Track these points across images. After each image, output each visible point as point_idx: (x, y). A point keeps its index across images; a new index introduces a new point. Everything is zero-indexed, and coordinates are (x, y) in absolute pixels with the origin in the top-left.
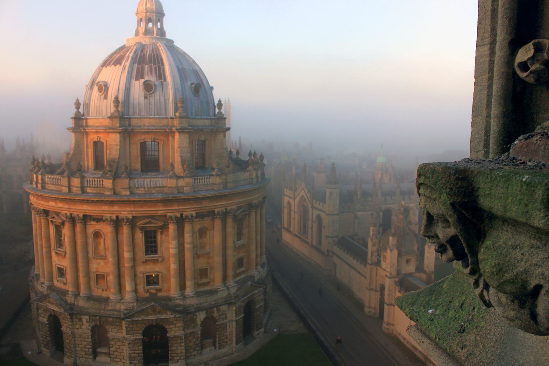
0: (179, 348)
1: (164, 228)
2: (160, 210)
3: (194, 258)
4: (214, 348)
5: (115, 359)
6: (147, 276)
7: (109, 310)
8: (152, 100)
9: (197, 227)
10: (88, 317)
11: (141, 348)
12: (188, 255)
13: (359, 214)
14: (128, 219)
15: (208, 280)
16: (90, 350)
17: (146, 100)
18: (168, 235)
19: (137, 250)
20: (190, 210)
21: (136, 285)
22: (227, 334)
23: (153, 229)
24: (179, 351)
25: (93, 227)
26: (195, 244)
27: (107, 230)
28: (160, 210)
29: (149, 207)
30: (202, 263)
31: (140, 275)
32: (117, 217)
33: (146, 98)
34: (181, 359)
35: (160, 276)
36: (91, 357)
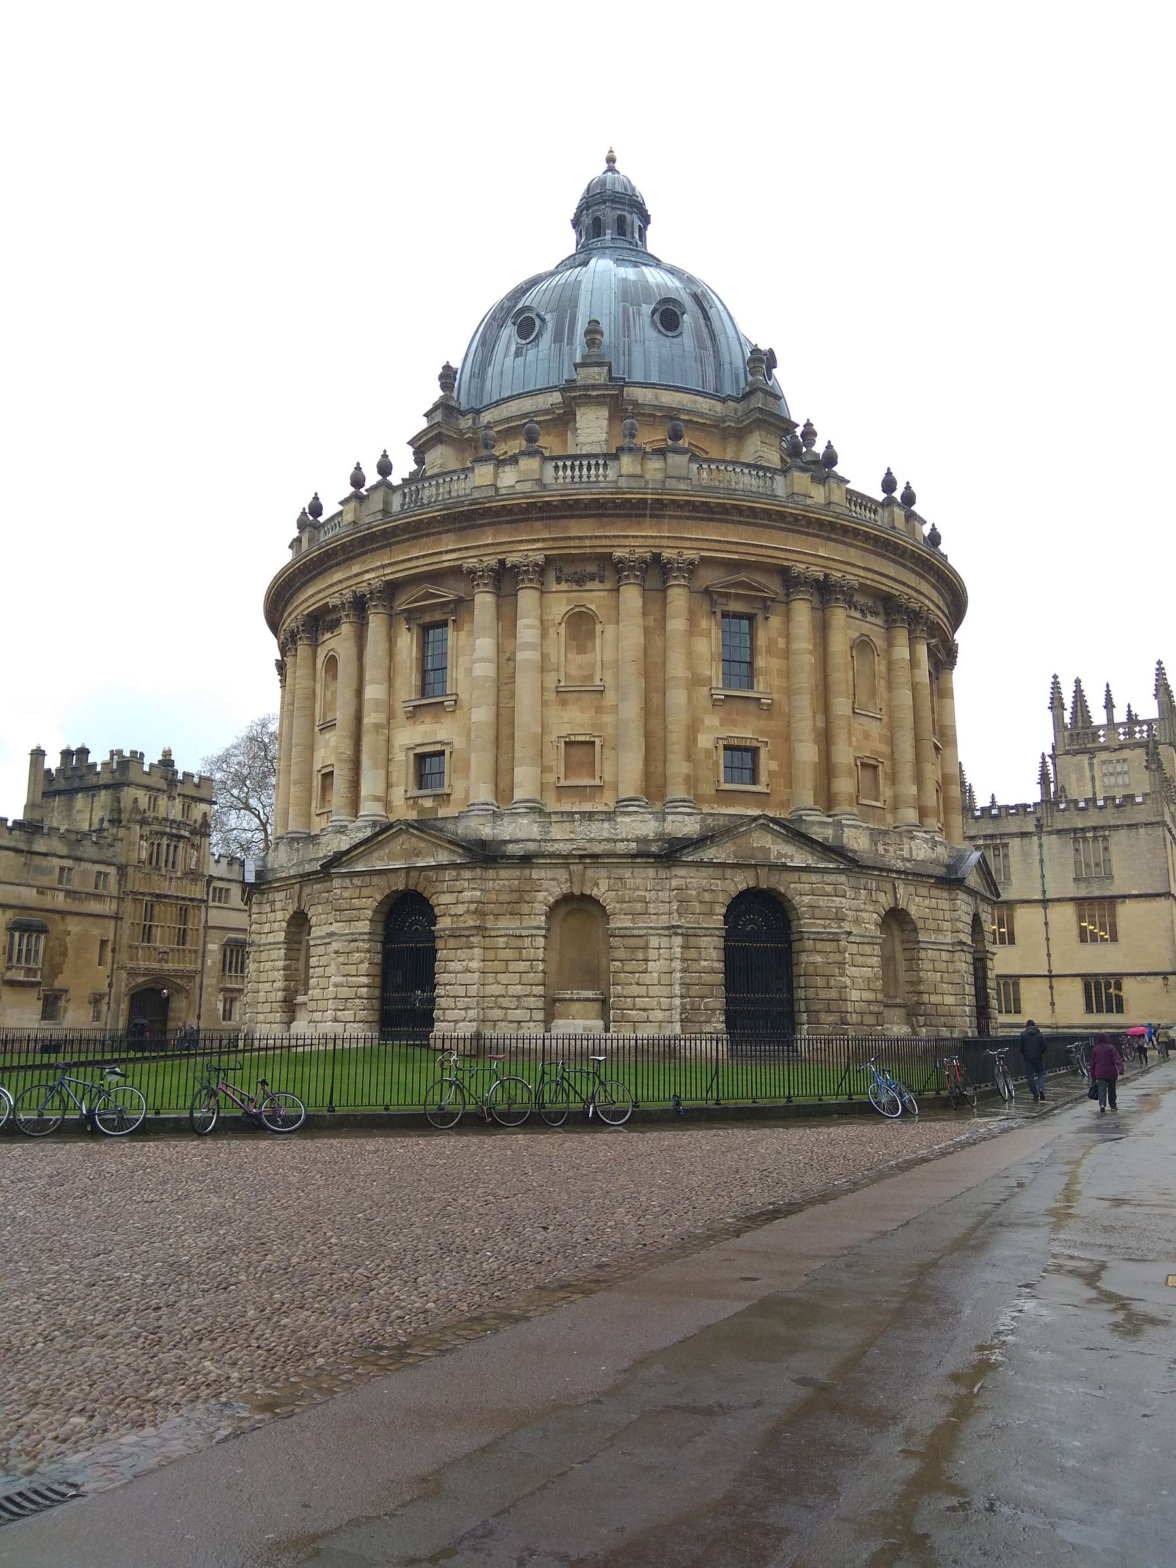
1: (462, 605)
2: (446, 551)
3: (544, 703)
4: (600, 1023)
8: (531, 354)
9: (559, 606)
12: (526, 685)
15: (597, 782)
16: (280, 995)
17: (520, 360)
18: (471, 633)
19: (399, 683)
20: (526, 546)
21: (389, 786)
22: (646, 979)
23: (438, 616)
24: (461, 991)
26: (554, 659)
28: (446, 551)
29: (422, 549)
30: (573, 720)
31: (399, 756)
32: (354, 592)
33: (518, 354)
35: (447, 753)
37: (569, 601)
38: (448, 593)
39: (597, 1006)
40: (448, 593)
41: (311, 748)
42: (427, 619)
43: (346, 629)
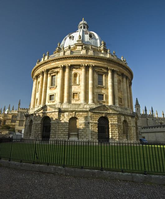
0: (115, 132)
5: (82, 137)
6: (99, 94)
7: (81, 108)
10: (68, 113)
11: (97, 129)
13: (148, 118)
14: (92, 66)
16: (67, 133)
21: (94, 98)
23: (102, 74)
25: (74, 71)
27: (81, 72)
31: (95, 94)
32: (88, 65)
34: (116, 138)
36: (67, 137)
37: (118, 78)
38: (105, 71)
39: (126, 137)
40: (105, 71)
41: (70, 87)
42: (100, 73)
43: (83, 70)
